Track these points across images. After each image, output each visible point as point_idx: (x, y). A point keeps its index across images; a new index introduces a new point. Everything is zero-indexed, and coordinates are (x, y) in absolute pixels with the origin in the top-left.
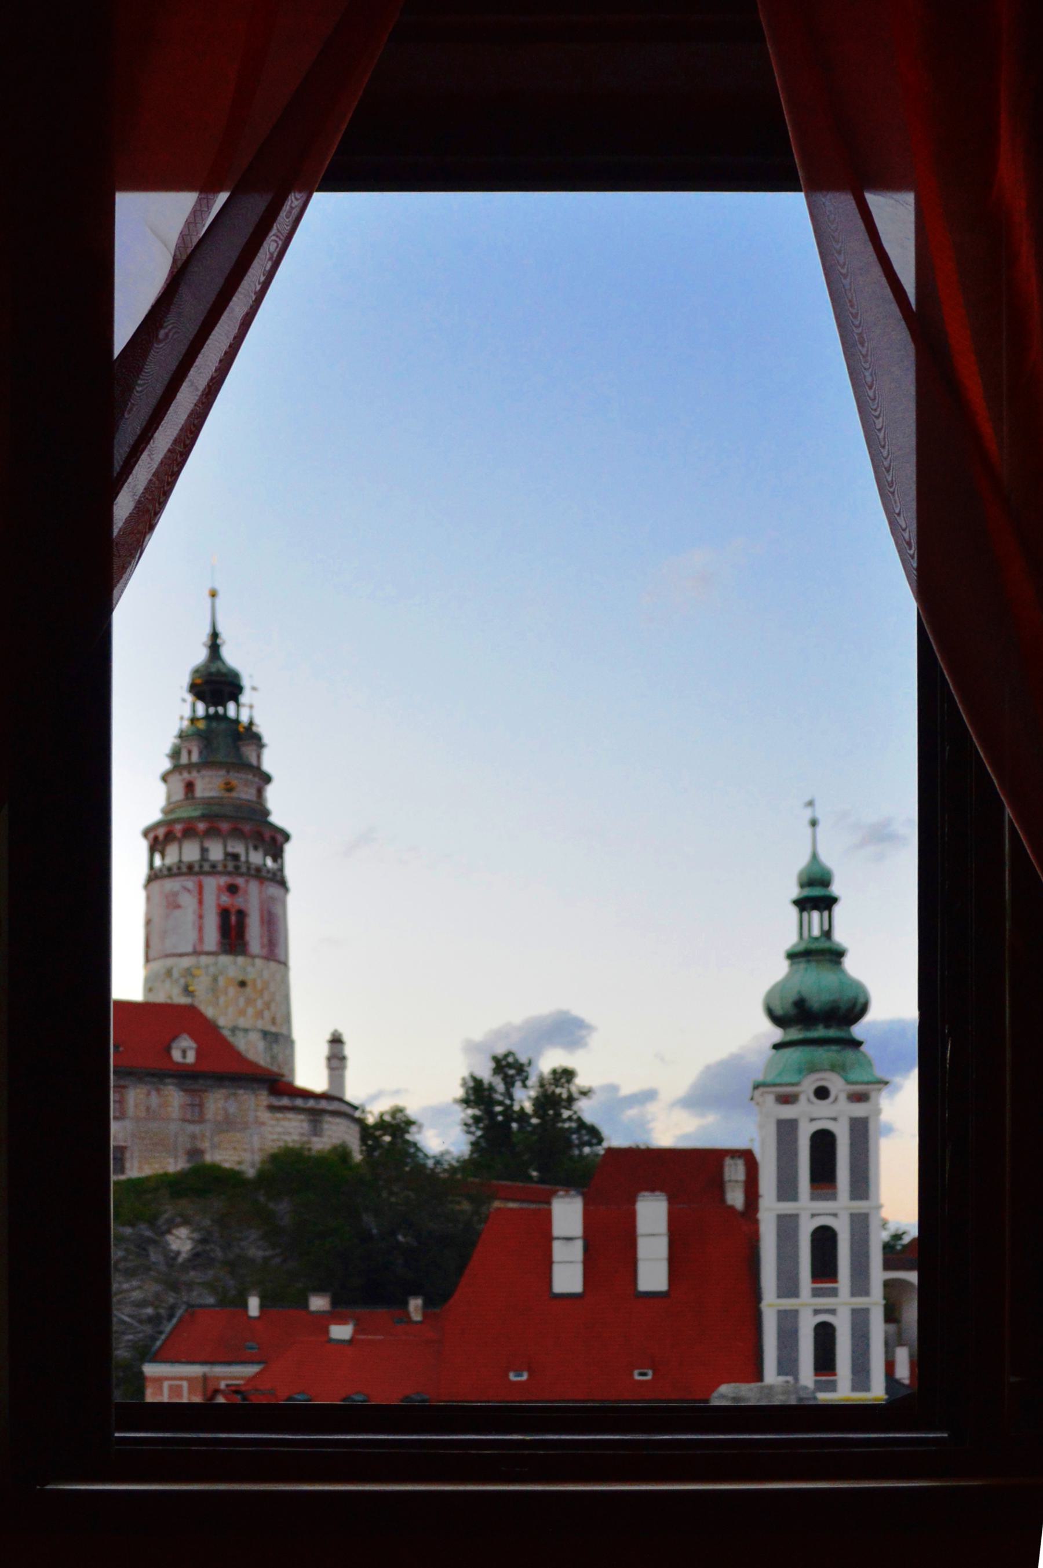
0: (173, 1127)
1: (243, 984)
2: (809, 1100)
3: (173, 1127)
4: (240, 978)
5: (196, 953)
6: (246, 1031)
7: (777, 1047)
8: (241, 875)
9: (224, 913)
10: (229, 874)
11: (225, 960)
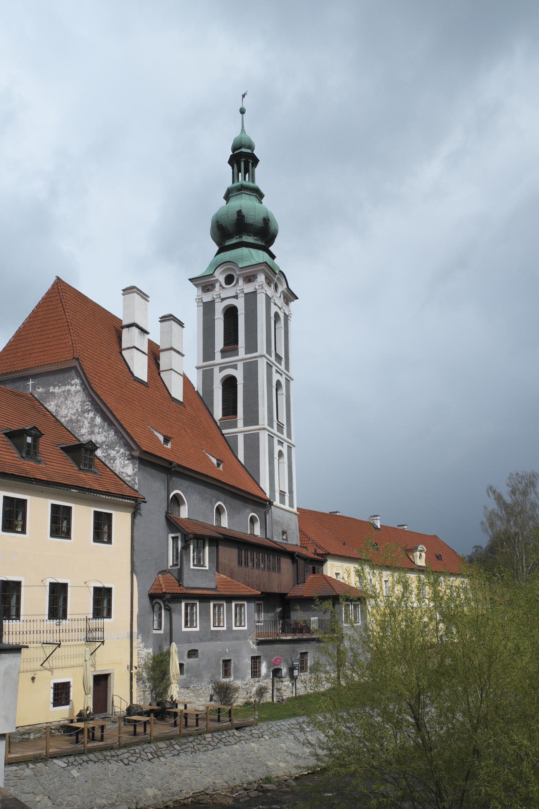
2: (221, 285)
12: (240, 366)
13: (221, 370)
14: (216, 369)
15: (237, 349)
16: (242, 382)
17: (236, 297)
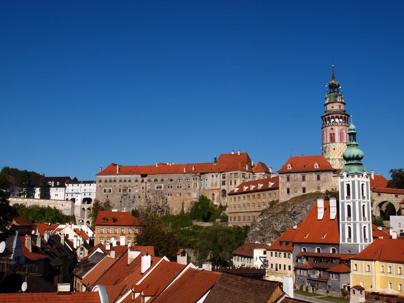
0: (315, 182)
1: (334, 149)
3: (315, 182)
4: (334, 148)
5: (326, 143)
6: (335, 159)
7: (345, 165)
8: (334, 126)
9: (331, 134)
10: (331, 126)
11: (331, 144)
12: (352, 202)
13: (347, 203)
14: (345, 203)
15: (350, 197)
16: (352, 207)
17: (349, 181)
